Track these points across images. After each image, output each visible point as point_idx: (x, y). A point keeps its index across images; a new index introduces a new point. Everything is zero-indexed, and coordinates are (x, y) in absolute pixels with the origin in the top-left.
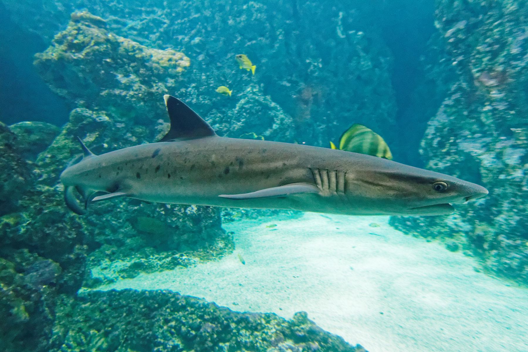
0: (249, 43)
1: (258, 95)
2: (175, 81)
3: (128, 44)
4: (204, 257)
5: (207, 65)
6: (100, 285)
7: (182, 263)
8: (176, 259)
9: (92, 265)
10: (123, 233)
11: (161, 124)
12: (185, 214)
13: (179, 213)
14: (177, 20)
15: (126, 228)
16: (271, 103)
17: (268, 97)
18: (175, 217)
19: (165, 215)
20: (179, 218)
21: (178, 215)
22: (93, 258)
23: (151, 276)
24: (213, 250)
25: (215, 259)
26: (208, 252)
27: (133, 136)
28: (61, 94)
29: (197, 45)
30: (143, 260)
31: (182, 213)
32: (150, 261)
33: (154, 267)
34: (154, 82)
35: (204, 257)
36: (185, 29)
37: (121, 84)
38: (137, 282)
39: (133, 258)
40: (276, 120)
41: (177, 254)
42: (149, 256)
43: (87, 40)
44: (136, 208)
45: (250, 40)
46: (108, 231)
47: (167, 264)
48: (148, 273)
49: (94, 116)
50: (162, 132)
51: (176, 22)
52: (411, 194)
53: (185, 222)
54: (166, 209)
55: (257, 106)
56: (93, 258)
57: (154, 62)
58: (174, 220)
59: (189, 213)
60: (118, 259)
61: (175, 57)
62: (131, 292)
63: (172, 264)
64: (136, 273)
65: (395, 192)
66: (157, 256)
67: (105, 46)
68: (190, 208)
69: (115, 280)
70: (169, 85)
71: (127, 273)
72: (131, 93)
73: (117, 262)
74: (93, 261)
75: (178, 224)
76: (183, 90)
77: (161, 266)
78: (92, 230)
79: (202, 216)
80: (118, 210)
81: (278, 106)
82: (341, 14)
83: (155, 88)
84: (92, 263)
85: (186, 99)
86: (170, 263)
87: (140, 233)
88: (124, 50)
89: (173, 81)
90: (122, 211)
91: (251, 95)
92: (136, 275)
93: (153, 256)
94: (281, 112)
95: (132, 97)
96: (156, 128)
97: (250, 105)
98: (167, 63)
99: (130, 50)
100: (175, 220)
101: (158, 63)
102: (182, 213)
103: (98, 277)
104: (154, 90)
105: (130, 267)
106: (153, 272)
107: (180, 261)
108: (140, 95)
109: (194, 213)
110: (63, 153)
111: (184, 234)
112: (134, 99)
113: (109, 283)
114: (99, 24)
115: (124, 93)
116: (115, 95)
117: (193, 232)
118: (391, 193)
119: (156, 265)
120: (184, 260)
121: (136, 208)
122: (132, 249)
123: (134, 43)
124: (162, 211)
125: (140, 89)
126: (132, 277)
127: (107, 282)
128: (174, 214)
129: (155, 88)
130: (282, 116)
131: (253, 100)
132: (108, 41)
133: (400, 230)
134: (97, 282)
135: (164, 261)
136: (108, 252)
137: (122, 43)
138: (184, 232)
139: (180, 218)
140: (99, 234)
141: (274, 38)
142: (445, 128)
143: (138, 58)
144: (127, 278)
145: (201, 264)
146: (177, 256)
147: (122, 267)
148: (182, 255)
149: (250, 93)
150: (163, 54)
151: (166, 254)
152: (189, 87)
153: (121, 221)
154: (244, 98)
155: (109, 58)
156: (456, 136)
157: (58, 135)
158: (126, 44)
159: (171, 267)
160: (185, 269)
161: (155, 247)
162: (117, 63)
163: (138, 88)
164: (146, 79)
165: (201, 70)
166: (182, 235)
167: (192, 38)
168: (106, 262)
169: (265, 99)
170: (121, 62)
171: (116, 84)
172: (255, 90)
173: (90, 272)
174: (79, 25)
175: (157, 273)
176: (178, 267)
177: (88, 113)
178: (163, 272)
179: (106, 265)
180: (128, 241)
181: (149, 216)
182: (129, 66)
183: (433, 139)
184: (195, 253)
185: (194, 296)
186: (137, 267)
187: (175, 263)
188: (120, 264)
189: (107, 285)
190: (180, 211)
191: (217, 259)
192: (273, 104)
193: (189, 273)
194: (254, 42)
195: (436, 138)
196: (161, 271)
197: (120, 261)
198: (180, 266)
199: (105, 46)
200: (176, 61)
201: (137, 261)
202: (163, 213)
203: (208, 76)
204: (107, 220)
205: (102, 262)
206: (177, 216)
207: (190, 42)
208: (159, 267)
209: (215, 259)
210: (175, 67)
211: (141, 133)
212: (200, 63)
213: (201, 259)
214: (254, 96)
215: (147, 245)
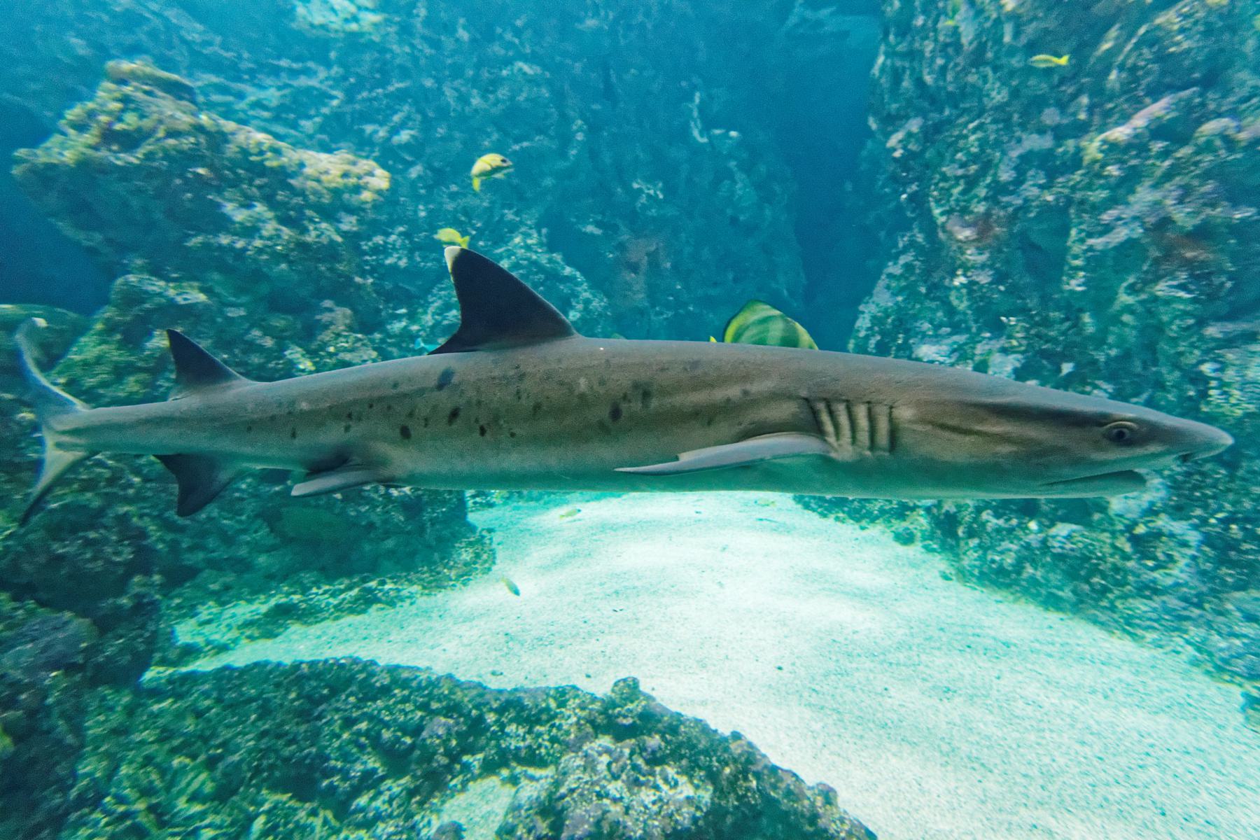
0: (517, 147)
1: (536, 252)
2: (358, 220)
3: (247, 138)
5: (429, 188)
6: (197, 658)
7: (383, 598)
8: (370, 590)
9: (177, 618)
10: (248, 543)
11: (330, 310)
12: (387, 496)
13: (375, 496)
14: (359, 92)
15: (256, 532)
16: (564, 269)
17: (558, 257)
19: (342, 501)
20: (374, 507)
21: (373, 499)
22: (177, 601)
23: (315, 630)
24: (450, 569)
25: (453, 585)
27: (265, 335)
28: (86, 243)
29: (406, 147)
30: (296, 598)
31: (381, 496)
32: (312, 599)
33: (321, 610)
34: (311, 220)
36: (378, 111)
37: (233, 223)
38: (284, 646)
39: (274, 596)
40: (574, 304)
41: (372, 580)
42: (310, 588)
43: (147, 123)
44: (277, 489)
45: (517, 140)
46: (211, 542)
47: (350, 602)
48: (311, 624)
49: (171, 293)
50: (333, 327)
51: (359, 97)
52: (1054, 450)
55: (537, 273)
56: (177, 601)
57: (308, 178)
60: (241, 599)
61: (355, 170)
62: (269, 668)
64: (281, 626)
65: (1014, 448)
66: (327, 587)
67: (192, 140)
69: (232, 645)
70: (345, 227)
71: (259, 627)
72: (258, 243)
73: (234, 606)
74: (179, 607)
75: (375, 518)
76: (379, 239)
77: (335, 607)
78: (173, 540)
79: (425, 498)
80: (237, 495)
81: (578, 274)
82: (697, 98)
83: (313, 234)
84: (176, 613)
85: (386, 258)
87: (287, 541)
88: (237, 150)
89: (353, 219)
90: (245, 496)
91: (523, 251)
92: (281, 630)
93: (319, 588)
94: (585, 286)
95: (260, 251)
96: (318, 317)
97: (521, 271)
98: (340, 180)
99: (253, 151)
101: (318, 181)
102: (381, 496)
103: (191, 642)
104: (310, 238)
105: (266, 615)
106: (319, 622)
107: (380, 595)
108: (279, 248)
110: (98, 374)
111: (388, 538)
112: (265, 257)
113: (218, 653)
114: (177, 90)
115: (240, 244)
116: (220, 247)
118: (1005, 449)
120: (388, 592)
121: (277, 489)
122: (271, 577)
123: (261, 136)
125: (279, 236)
126: (270, 635)
127: (213, 651)
128: (363, 498)
129: (313, 234)
130: (587, 295)
131: (525, 262)
132: (199, 129)
133: (814, 511)
134: (190, 652)
135: (343, 596)
136: (213, 587)
137: (233, 134)
138: (387, 534)
139: (378, 507)
140: (191, 549)
141: (566, 140)
142: (888, 317)
143: (272, 169)
144: (258, 638)
145: (425, 598)
146: (373, 584)
147: (248, 617)
148: (383, 583)
149: (521, 247)
150: (330, 162)
151: (347, 582)
152: (391, 233)
153: (244, 518)
154: (509, 257)
155: (203, 166)
156: (906, 331)
157: (82, 334)
158: (241, 138)
159: (358, 609)
161: (323, 569)
162: (221, 178)
163: (274, 233)
164: (292, 213)
165: (417, 198)
166: (383, 540)
167: (395, 130)
168: (210, 607)
169: (550, 261)
170: (231, 176)
171: (224, 223)
172: (529, 242)
173: (172, 632)
174: (128, 89)
175: (328, 623)
176: (375, 607)
177: (156, 285)
178: (342, 621)
179: (210, 614)
180: (262, 560)
182: (251, 184)
183: (867, 338)
184: (413, 576)
185: (410, 664)
186: (284, 613)
187: (367, 600)
188: (244, 610)
189: (212, 657)
190: (377, 491)
191: (459, 585)
192: (568, 271)
193: (399, 616)
194: (525, 144)
195: (873, 335)
196: (337, 618)
197: (243, 603)
198: (379, 606)
199: (192, 140)
200: (359, 177)
201: (284, 600)
203: (430, 212)
204: (210, 519)
205: (200, 608)
206: (369, 501)
207: (389, 139)
208: (332, 610)
209: (453, 585)
210: (357, 189)
211: (283, 331)
212: (413, 184)
213: (424, 588)
214: (529, 254)
215: (306, 567)
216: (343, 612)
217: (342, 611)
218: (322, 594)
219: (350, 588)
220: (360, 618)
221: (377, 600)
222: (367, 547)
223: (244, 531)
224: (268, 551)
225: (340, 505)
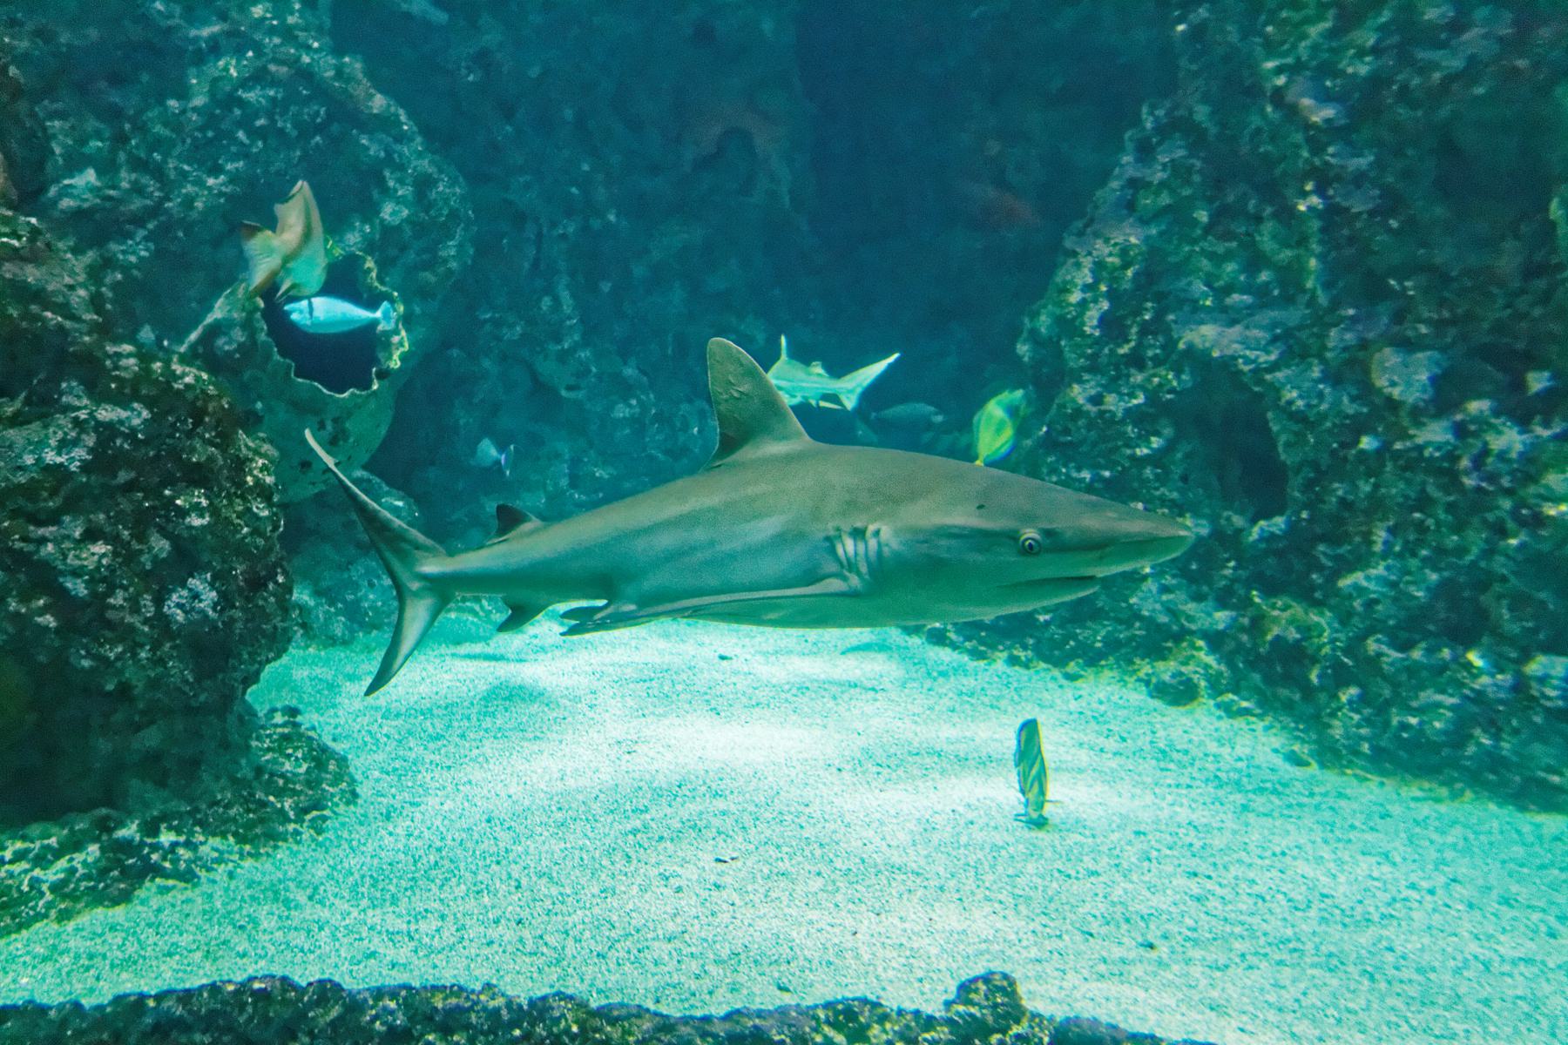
4: (250, 826)
7: (167, 865)
12: (161, 621)
21: (132, 629)
26: (264, 804)
31: (146, 621)
33: (24, 898)
35: (250, 826)
47: (87, 877)
53: (161, 662)
58: (112, 656)
59: (180, 616)
63: (116, 873)
68: (185, 593)
77: (55, 888)
86: (103, 873)
109: (206, 616)
111: (152, 722)
119: (32, 887)
124: (42, 611)
128: (109, 625)
138: (151, 715)
139: (142, 646)
142: (1126, 266)
148: (151, 829)
159: (113, 891)
160: (180, 892)
166: (138, 728)
190: (135, 608)
196: (64, 916)
202: (49, 620)
206: (126, 634)
208: (49, 896)
216: (76, 899)
217: (73, 897)
218: (11, 862)
219: (74, 844)
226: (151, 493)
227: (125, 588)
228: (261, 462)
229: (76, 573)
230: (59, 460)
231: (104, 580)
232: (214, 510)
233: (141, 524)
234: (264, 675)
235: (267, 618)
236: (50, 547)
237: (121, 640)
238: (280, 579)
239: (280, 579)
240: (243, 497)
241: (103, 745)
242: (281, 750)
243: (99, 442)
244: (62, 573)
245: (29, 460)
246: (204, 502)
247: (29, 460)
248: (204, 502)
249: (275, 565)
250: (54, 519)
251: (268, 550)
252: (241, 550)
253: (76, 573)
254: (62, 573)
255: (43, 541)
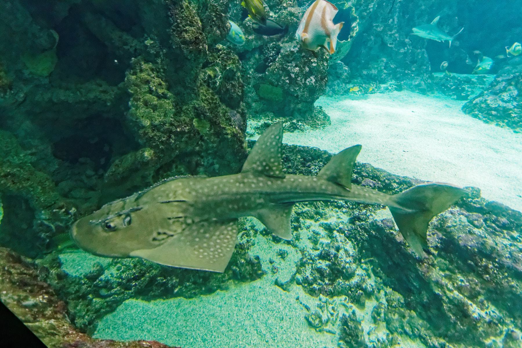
12: (305, 84)
18: (297, 87)
19: (289, 84)
21: (300, 85)
26: (316, 122)
31: (303, 84)
53: (304, 92)
54: (290, 78)
59: (308, 84)
68: (310, 79)
75: (299, 93)
100: (298, 90)
102: (303, 84)
105: (261, 126)
117: (306, 102)
128: (297, 83)
139: (301, 88)
161: (273, 112)
176: (296, 131)
180: (254, 105)
181: (272, 84)
184: (307, 121)
190: (301, 81)
202: (288, 81)
213: (311, 127)
215: (268, 110)
220: (292, 134)
221: (298, 128)
222: (292, 106)
223: (249, 92)
224: (255, 102)
225: (288, 85)
226: (308, 58)
227: (300, 77)
228: (327, 53)
229: (293, 73)
230: (293, 50)
231: (297, 75)
232: (317, 63)
233: (305, 64)
234: (320, 98)
235: (322, 86)
236: (290, 68)
237: (299, 87)
238: (326, 79)
239: (326, 79)
240: (323, 61)
241: (292, 106)
242: (319, 113)
243: (300, 47)
244: (291, 73)
245: (288, 50)
246: (316, 61)
247: (288, 50)
248: (316, 61)
249: (326, 76)
250: (291, 62)
251: (325, 73)
252: (320, 72)
253: (293, 73)
254: (291, 73)
255: (289, 66)
